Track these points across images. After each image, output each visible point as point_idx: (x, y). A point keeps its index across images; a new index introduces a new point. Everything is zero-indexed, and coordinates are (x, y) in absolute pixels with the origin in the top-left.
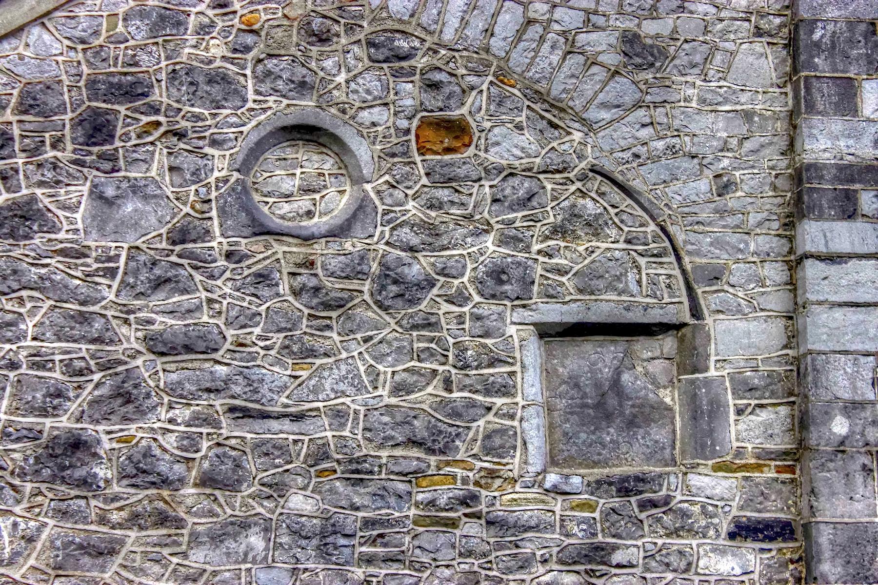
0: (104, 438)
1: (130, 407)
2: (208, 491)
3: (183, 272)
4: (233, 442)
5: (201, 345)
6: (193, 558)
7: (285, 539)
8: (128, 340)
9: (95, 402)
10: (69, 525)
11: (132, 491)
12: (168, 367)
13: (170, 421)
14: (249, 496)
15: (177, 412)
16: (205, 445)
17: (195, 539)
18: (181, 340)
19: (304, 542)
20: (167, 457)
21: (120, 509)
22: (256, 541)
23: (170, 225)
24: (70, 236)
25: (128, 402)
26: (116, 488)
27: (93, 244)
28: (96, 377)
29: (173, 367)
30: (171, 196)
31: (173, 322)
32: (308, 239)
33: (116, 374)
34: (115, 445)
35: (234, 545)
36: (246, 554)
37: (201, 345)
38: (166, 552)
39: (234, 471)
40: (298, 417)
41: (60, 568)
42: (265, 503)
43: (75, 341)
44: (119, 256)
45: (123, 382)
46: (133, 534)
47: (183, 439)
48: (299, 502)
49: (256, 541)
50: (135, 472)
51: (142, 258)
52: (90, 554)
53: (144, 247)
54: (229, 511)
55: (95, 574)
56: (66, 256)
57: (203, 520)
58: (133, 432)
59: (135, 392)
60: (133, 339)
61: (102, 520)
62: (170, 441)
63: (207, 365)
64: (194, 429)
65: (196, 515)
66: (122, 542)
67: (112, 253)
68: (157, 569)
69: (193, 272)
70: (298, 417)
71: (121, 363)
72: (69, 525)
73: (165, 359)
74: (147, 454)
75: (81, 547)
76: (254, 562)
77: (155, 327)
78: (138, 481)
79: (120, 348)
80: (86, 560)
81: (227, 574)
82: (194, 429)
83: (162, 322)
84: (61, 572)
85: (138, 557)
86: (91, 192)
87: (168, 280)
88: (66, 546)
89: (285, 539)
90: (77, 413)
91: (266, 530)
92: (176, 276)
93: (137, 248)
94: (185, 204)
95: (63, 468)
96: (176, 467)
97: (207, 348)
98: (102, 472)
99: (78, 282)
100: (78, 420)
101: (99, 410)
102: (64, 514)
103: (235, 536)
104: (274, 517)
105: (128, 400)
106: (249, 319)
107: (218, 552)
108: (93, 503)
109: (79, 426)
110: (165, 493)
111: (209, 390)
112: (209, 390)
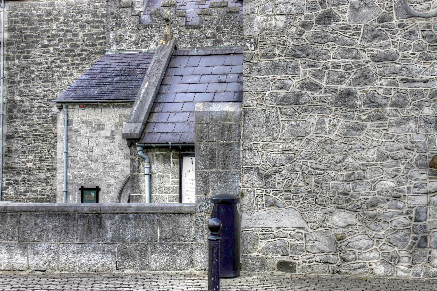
0: (358, 91)
1: (367, 80)
2: (395, 108)
3: (383, 32)
4: (403, 91)
5: (391, 58)
6: (390, 131)
7: (422, 124)
8: (365, 57)
9: (355, 79)
10: (348, 121)
11: (369, 109)
12: (379, 66)
13: (381, 84)
14: (409, 109)
15: (383, 81)
16: (393, 92)
17: (391, 125)
18: (383, 56)
19: (429, 125)
20: (380, 97)
21: (365, 115)
22: (412, 125)
23: (378, 16)
24: (344, 22)
25: (366, 78)
26: (363, 108)
27: (352, 25)
28: (355, 70)
29: (381, 66)
30: (378, 6)
31: (380, 50)
32: (428, 18)
33: (362, 69)
34: (362, 93)
35: (405, 126)
36: (409, 129)
37: (391, 58)
38: (381, 129)
39: (404, 101)
40: (426, 81)
41: (345, 135)
42: (415, 112)
43: (347, 58)
44: (361, 28)
45: (364, 72)
46: (369, 123)
47: (385, 90)
48: (427, 111)
49: (412, 125)
50: (369, 102)
51: (369, 28)
52: (355, 130)
53: (369, 24)
54: (402, 115)
55: (357, 137)
56: (343, 29)
57: (393, 118)
58: (368, 89)
59: (368, 75)
60: (367, 57)
61: (359, 119)
62: (381, 91)
63: (393, 65)
64: (389, 87)
65: (391, 116)
66: (366, 126)
67: (358, 27)
68: (378, 135)
69: (387, 32)
70: (426, 81)
71: (363, 65)
72: (348, 121)
73: (378, 63)
74: (373, 96)
75: (352, 128)
76: (412, 132)
77: (374, 52)
78: (371, 105)
79: (362, 60)
80: (354, 132)
81: (402, 136)
82: (389, 87)
83: (376, 50)
84: (346, 136)
85: (371, 131)
86: (350, 7)
87: (378, 36)
88: (347, 127)
89: (422, 124)
90: (349, 83)
91: (416, 121)
92: (381, 34)
93: (367, 25)
94: (383, 8)
95: (345, 102)
96: (383, 100)
97: (393, 58)
98: (358, 102)
99: (347, 38)
100: (349, 85)
101: (356, 81)
102: (346, 117)
103: (405, 123)
104: (418, 117)
105: (366, 77)
106: (406, 48)
107: (399, 129)
108: (355, 113)
109: (350, 87)
110: (380, 109)
111: (394, 73)
112: (394, 73)
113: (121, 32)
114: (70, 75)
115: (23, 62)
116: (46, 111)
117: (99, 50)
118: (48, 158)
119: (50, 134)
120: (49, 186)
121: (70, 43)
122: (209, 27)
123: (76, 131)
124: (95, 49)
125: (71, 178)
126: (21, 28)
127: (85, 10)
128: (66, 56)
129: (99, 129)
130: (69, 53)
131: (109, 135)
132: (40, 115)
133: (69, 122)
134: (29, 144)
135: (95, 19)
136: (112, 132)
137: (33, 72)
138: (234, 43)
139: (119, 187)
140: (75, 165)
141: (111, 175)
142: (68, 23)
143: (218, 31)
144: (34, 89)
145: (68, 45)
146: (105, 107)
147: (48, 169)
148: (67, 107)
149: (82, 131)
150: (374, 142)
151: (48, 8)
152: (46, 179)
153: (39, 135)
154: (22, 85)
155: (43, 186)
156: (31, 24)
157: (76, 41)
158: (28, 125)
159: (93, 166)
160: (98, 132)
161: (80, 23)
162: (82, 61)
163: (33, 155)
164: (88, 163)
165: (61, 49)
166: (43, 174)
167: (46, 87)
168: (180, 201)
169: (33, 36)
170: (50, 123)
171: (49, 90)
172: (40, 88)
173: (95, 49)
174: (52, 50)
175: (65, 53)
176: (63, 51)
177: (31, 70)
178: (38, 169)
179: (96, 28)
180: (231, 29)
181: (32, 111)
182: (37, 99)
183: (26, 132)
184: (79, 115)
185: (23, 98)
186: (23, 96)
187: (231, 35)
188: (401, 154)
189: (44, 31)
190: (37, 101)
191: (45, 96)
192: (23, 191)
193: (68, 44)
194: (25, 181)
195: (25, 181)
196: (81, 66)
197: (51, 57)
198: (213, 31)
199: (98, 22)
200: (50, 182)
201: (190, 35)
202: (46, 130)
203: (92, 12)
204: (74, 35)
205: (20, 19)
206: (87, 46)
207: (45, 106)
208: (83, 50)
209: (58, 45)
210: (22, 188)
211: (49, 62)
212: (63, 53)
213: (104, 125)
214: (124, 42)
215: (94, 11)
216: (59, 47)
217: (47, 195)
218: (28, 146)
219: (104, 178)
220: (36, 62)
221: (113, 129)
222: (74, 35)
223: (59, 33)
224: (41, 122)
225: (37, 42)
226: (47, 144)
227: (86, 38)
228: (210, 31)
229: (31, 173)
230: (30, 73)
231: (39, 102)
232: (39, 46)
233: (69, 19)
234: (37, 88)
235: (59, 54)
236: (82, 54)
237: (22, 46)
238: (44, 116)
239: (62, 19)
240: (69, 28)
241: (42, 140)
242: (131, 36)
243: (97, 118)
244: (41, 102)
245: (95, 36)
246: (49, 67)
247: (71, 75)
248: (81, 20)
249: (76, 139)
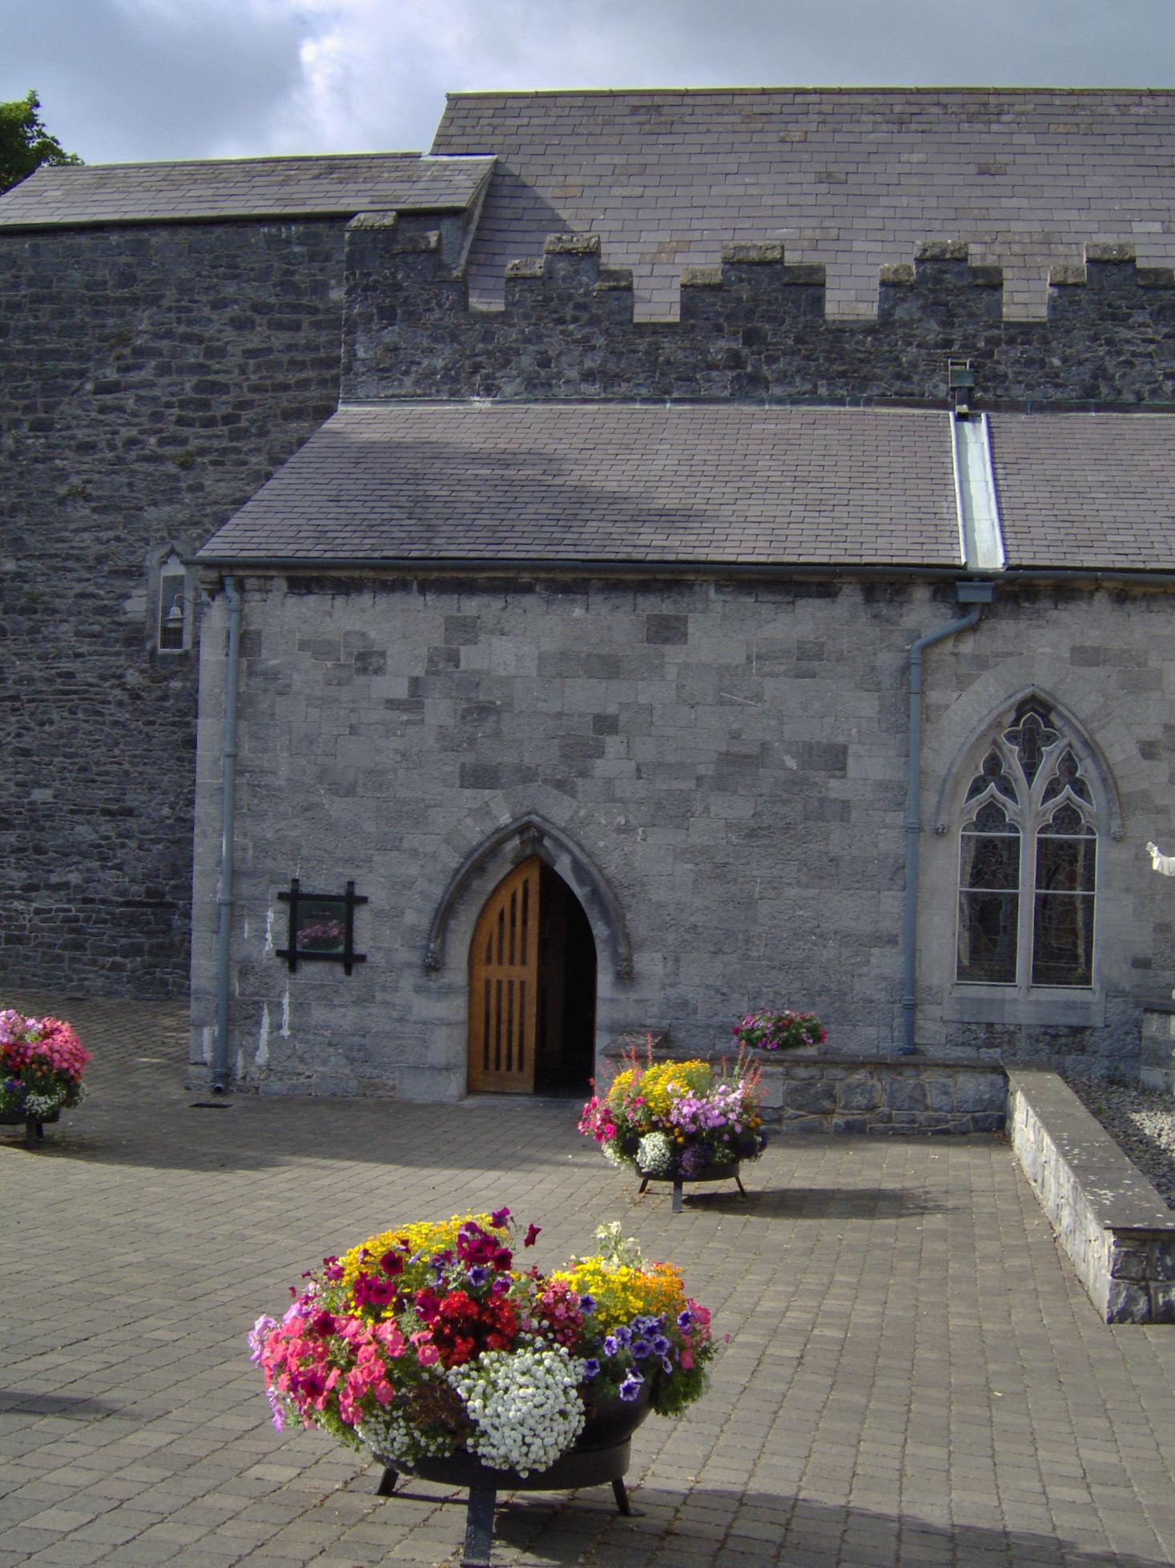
113: (396, 338)
114: (191, 489)
115: (30, 441)
116: (101, 611)
117: (294, 405)
118: (107, 773)
119: (117, 692)
120: (110, 868)
121: (195, 379)
122: (719, 329)
123: (273, 675)
124: (285, 400)
125: (251, 853)
126: (27, 328)
127: (252, 270)
128: (181, 421)
129: (364, 670)
130: (191, 414)
131: (401, 691)
132: (82, 623)
133: (246, 643)
134: (42, 724)
135: (290, 298)
136: (415, 682)
137: (62, 476)
138: (808, 387)
139: (437, 891)
140: (265, 806)
141: (406, 844)
142: (191, 311)
143: (750, 346)
144: (63, 534)
145: (188, 386)
146: (389, 587)
147: (106, 812)
148: (240, 587)
149: (296, 676)
151: (124, 259)
152: (100, 846)
153: (76, 692)
154: (21, 520)
155: (89, 870)
156: (61, 314)
157: (217, 372)
158: (40, 658)
159: (337, 808)
160: (359, 680)
161: (234, 310)
162: (237, 439)
163: (56, 760)
164: (316, 799)
165: (164, 399)
166: (90, 829)
167: (107, 529)
169: (68, 351)
170: (118, 654)
171: (118, 539)
172: (86, 530)
173: (285, 400)
174: (131, 402)
175: (176, 411)
176: (169, 405)
177: (59, 470)
178: (72, 812)
179: (289, 328)
180: (799, 340)
181: (54, 611)
182: (71, 570)
183: (31, 680)
184: (286, 617)
185: (24, 563)
186: (25, 557)
187: (797, 361)
189: (105, 339)
190: (75, 575)
191: (101, 559)
192: (17, 884)
193: (189, 383)
194: (25, 850)
195: (25, 850)
196: (235, 457)
197: (129, 424)
198: (734, 345)
199: (296, 308)
200: (115, 857)
201: (647, 353)
202: (104, 678)
203: (275, 277)
204: (210, 353)
205: (25, 296)
206: (255, 389)
207: (102, 592)
208: (243, 405)
209: (151, 385)
210: (15, 874)
211: (119, 441)
212: (171, 411)
213: (383, 654)
214: (406, 373)
215: (287, 272)
216: (157, 392)
217: (104, 901)
218: (37, 728)
219: (378, 858)
220: (72, 443)
221: (419, 671)
222: (210, 353)
223: (158, 344)
224: (84, 649)
225: (82, 374)
226: (104, 723)
227: (252, 362)
228: (722, 343)
229: (48, 824)
230: (54, 479)
231: (80, 580)
232: (89, 387)
233: (197, 297)
234: (76, 531)
235: (156, 417)
236: (237, 418)
237: (28, 386)
238: (97, 628)
239: (170, 296)
240: (196, 330)
241: (86, 711)
242: (431, 350)
243: (357, 628)
244: (88, 580)
245: (285, 358)
246: (120, 460)
247: (197, 488)
248: (236, 302)
249: (272, 706)
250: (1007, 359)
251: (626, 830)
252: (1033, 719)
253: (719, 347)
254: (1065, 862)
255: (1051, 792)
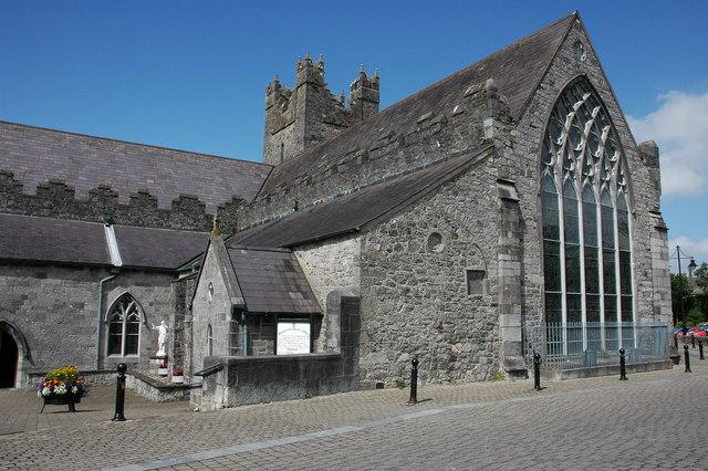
150: (417, 315)
168: (275, 353)
188: (427, 322)
250: (118, 213)
251: (29, 322)
252: (126, 299)
253: (46, 204)
254: (132, 328)
255: (130, 312)
